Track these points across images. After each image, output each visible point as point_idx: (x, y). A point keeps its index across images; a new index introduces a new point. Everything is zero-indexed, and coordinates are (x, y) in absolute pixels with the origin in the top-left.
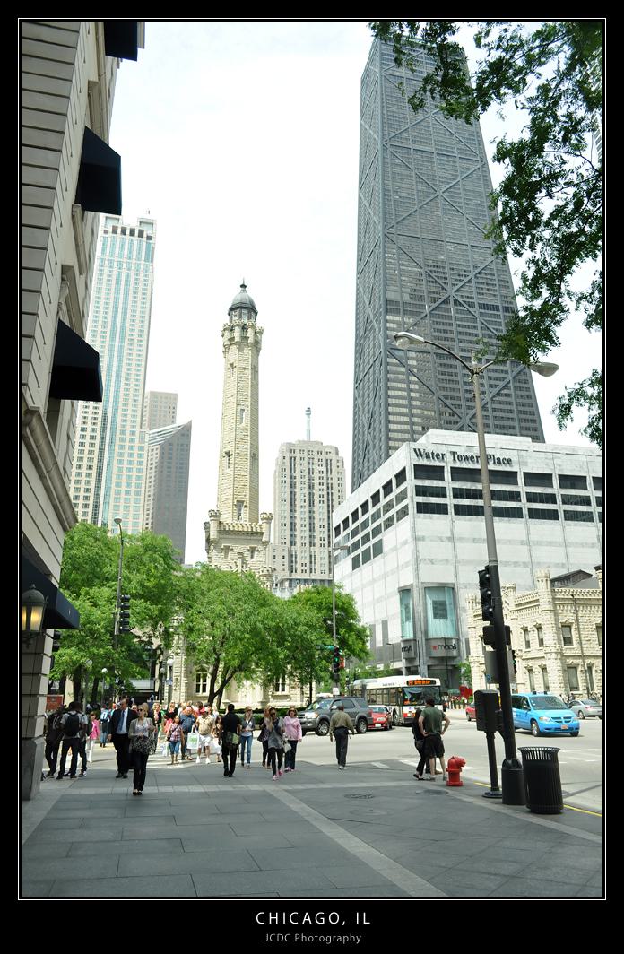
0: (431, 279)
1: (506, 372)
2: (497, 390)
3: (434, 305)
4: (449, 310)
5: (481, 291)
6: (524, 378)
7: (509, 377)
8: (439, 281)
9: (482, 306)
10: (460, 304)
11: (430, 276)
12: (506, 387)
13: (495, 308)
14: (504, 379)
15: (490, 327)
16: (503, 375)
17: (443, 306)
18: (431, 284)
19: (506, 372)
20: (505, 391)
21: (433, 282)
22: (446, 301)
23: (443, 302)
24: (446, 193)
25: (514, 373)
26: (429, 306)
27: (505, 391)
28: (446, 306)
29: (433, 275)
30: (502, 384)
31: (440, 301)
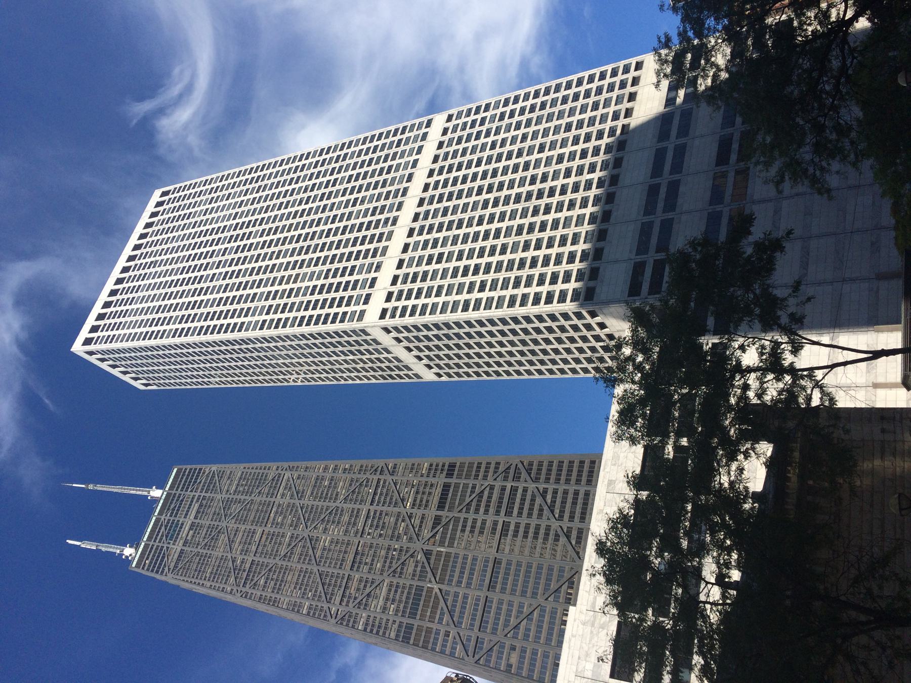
0: (399, 569)
1: (525, 490)
2: (545, 508)
3: (430, 575)
4: (439, 554)
5: (424, 502)
6: (535, 467)
7: (532, 486)
8: (403, 558)
9: (441, 507)
10: (434, 536)
11: (394, 571)
12: (544, 494)
13: (446, 487)
14: (533, 496)
15: (468, 500)
16: (529, 493)
17: (432, 561)
18: (405, 570)
19: (525, 490)
20: (549, 498)
21: (402, 569)
22: (427, 554)
23: (428, 559)
24: (309, 524)
25: (528, 478)
26: (430, 582)
27: (549, 498)
28: (433, 558)
29: (394, 566)
30: (539, 500)
31: (426, 565)
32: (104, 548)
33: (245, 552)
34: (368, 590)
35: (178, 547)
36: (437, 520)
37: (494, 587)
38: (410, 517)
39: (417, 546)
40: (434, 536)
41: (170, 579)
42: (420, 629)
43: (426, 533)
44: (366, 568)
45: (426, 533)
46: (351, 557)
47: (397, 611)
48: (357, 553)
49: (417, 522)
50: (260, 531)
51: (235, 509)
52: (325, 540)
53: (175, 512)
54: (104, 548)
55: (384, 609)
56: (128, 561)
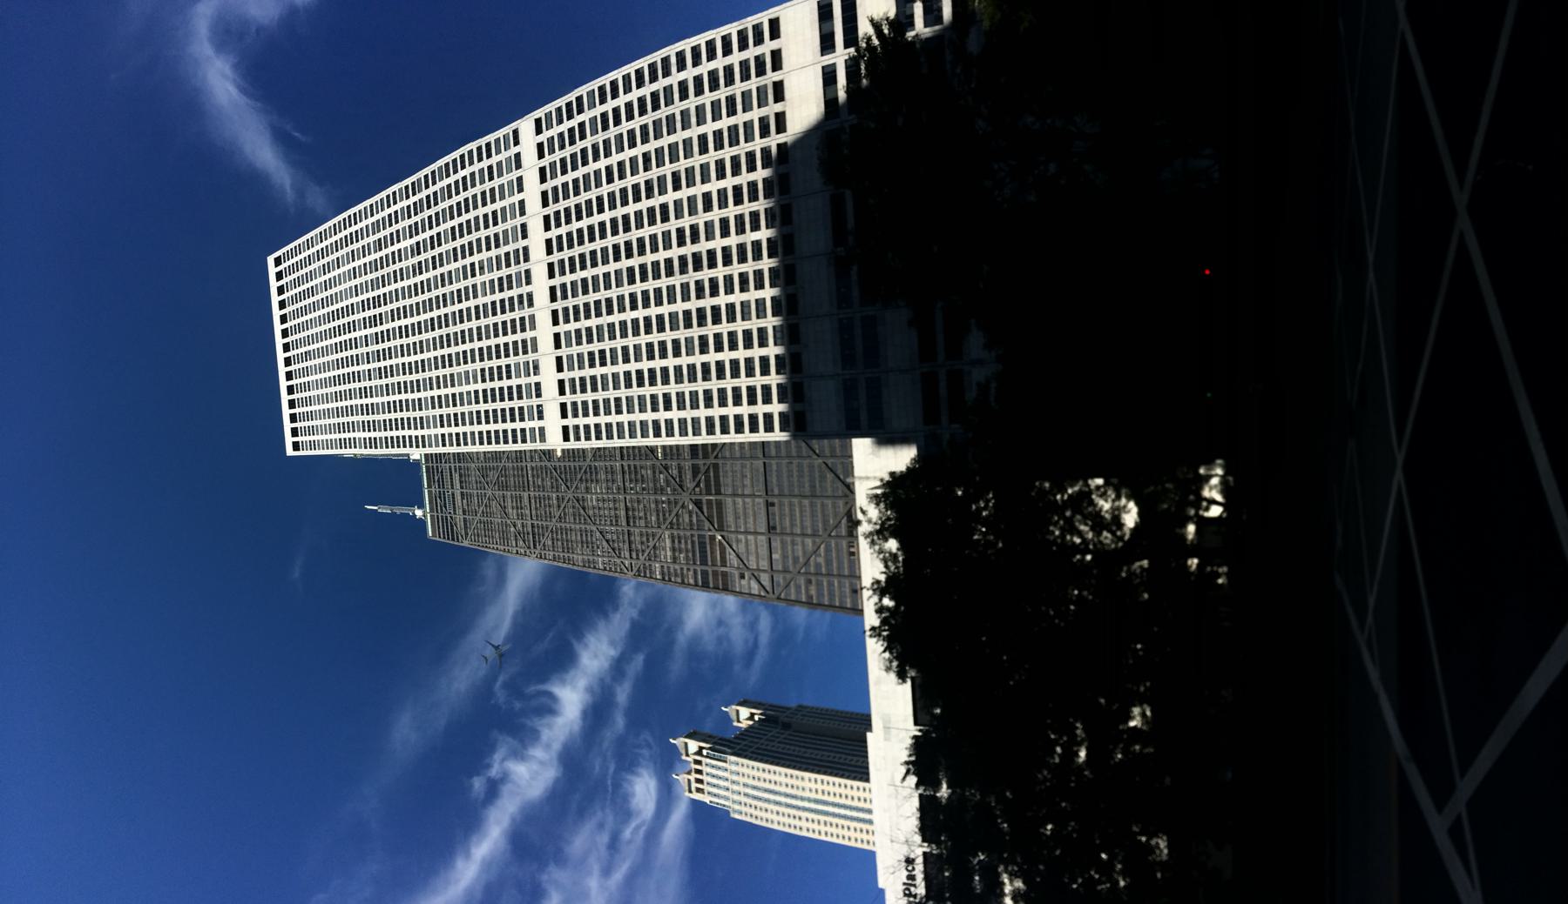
4: (709, 502)
10: (698, 485)
22: (698, 504)
32: (399, 510)
33: (521, 516)
34: (651, 544)
35: (459, 517)
36: (695, 470)
37: (774, 528)
38: (666, 468)
39: (685, 498)
40: (698, 485)
41: (466, 543)
42: (715, 573)
43: (690, 484)
44: (642, 523)
45: (690, 484)
46: (623, 513)
47: (687, 558)
48: (627, 509)
49: (675, 472)
50: (526, 495)
51: (493, 476)
52: (592, 500)
53: (441, 484)
54: (399, 510)
55: (675, 560)
56: (422, 522)
